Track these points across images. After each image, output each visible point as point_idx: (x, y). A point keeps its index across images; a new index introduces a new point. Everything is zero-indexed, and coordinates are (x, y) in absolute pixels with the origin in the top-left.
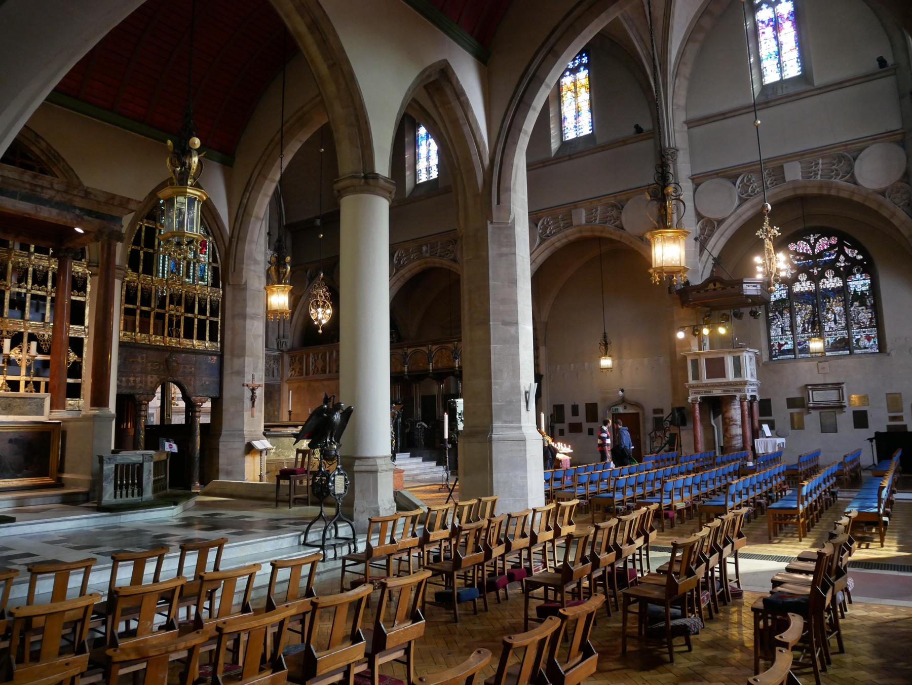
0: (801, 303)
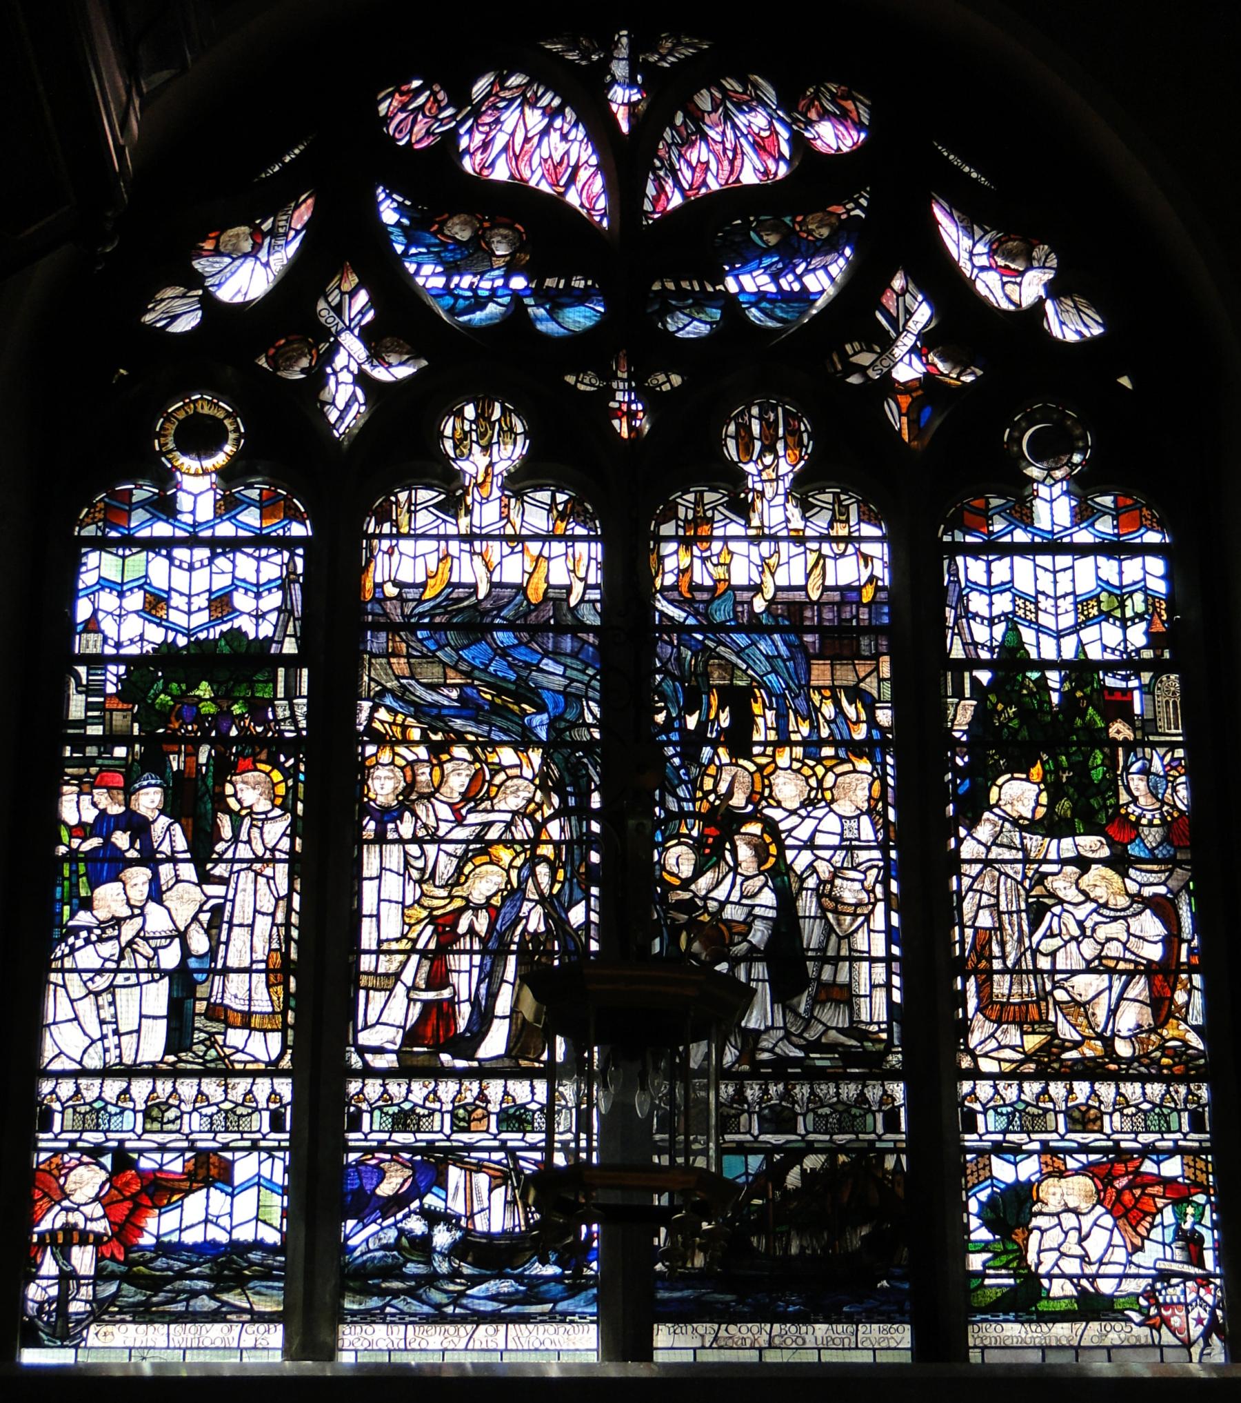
0: (429, 715)
